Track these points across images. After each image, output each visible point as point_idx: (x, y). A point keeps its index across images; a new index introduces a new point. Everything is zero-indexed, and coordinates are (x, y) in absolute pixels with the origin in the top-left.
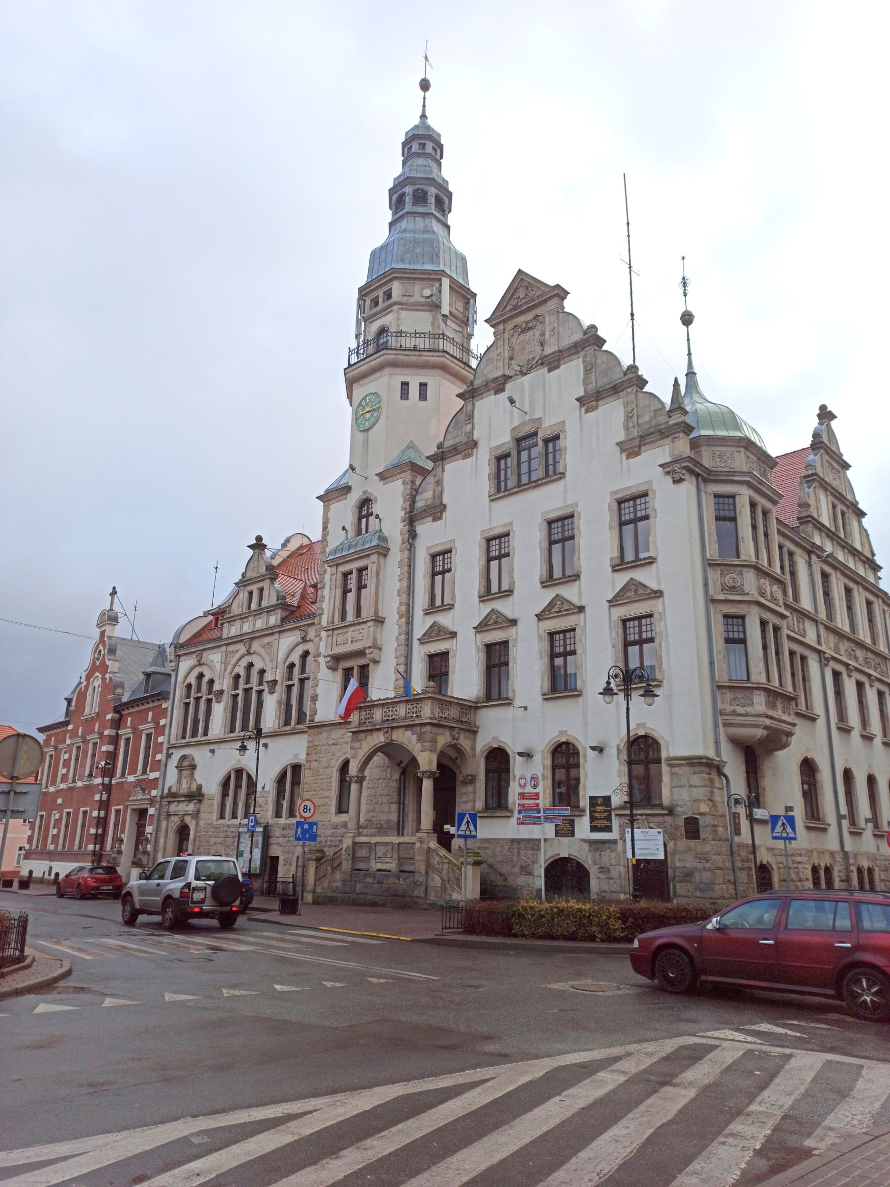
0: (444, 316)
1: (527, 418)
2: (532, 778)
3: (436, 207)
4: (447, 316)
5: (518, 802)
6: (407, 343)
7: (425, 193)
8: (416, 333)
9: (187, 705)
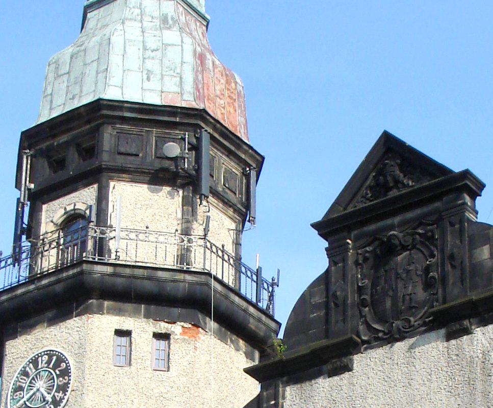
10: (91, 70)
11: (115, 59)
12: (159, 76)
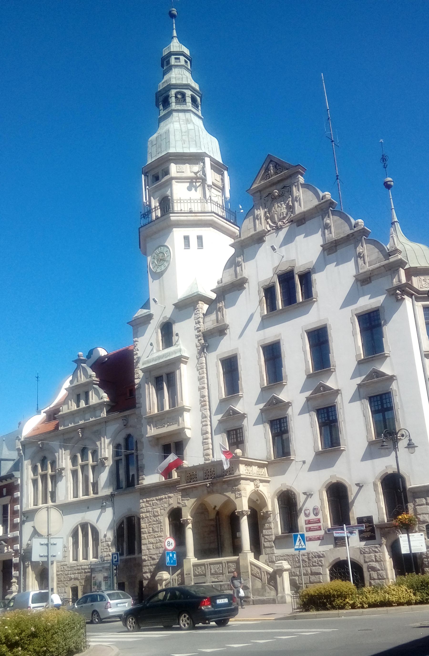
0: (209, 186)
1: (284, 259)
2: (314, 509)
3: (192, 104)
4: (211, 186)
5: (305, 526)
6: (186, 208)
7: (183, 95)
8: (190, 199)
9: (35, 482)
10: (163, 143)
11: (172, 137)
12: (188, 142)
